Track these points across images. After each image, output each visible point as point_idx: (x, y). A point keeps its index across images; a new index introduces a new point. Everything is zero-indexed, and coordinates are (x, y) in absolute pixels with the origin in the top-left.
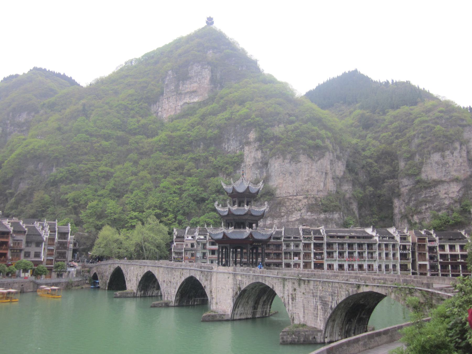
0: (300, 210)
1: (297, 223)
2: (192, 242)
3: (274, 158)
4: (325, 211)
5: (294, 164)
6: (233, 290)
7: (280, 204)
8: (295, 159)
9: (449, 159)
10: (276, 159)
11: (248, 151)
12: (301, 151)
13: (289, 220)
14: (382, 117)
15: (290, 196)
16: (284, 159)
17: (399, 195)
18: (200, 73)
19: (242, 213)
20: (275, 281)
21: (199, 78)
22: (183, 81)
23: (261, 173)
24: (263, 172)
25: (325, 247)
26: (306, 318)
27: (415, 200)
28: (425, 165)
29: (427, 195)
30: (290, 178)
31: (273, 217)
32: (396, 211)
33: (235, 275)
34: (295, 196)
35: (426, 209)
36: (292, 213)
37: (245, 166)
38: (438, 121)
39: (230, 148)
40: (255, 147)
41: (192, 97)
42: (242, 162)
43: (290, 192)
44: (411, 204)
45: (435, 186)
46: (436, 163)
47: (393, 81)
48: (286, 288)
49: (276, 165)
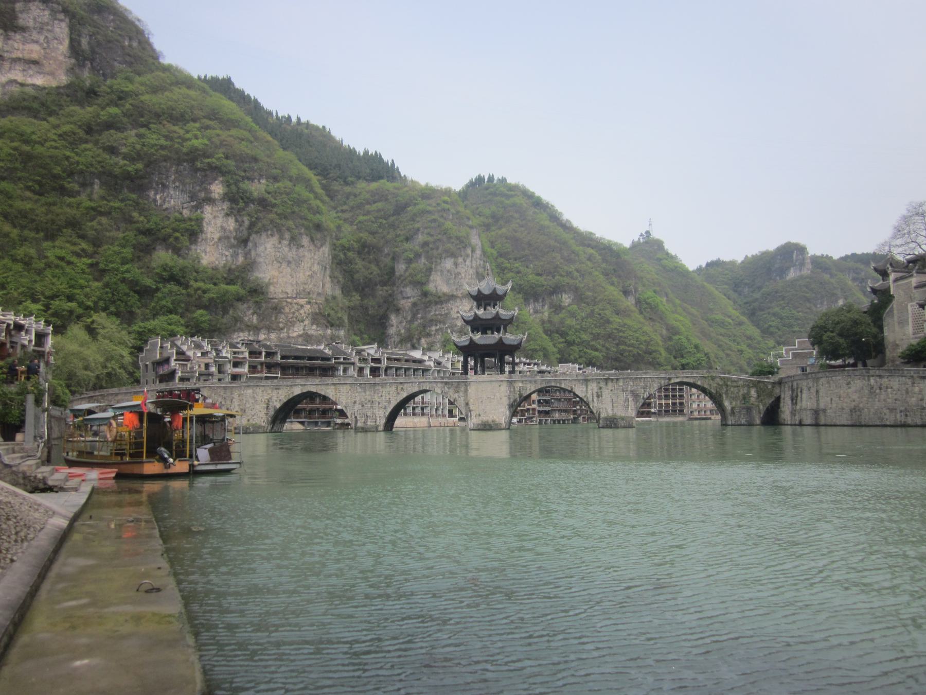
0: (303, 321)
1: (300, 340)
2: (206, 361)
3: (264, 235)
4: (332, 325)
5: (294, 249)
6: (509, 399)
7: (277, 309)
8: (294, 240)
9: (461, 269)
10: (267, 235)
11: (211, 214)
12: (303, 231)
13: (291, 335)
14: (348, 189)
15: (290, 298)
16: (281, 238)
17: (398, 310)
18: (49, 28)
19: (489, 317)
20: (574, 383)
21: (46, 37)
22: (6, 31)
23: (235, 255)
24: (238, 254)
25: (382, 372)
26: (615, 410)
27: (422, 318)
28: (433, 273)
29: (437, 313)
30: (288, 268)
31: (269, 329)
32: (392, 331)
33: (511, 383)
34: (295, 298)
35: (437, 330)
36: (293, 324)
37: (206, 240)
38: (445, 215)
39: (169, 202)
40: (223, 209)
41: (31, 72)
42: (202, 231)
43: (288, 291)
44: (416, 323)
45: (447, 301)
46: (448, 271)
47: (299, 119)
48: (590, 387)
49: (269, 246)
